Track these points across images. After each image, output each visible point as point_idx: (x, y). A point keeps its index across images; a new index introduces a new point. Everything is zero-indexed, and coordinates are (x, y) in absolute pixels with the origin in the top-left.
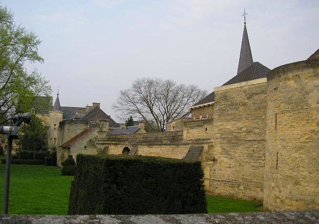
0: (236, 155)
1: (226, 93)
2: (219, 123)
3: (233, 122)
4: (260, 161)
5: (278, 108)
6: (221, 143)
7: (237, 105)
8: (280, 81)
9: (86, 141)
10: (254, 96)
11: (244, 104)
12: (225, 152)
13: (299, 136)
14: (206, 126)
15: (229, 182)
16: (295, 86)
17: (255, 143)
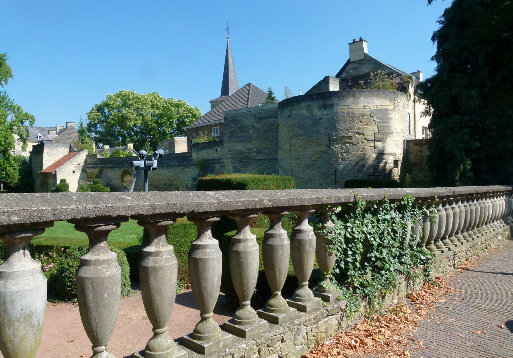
1: (236, 116)
2: (230, 145)
3: (243, 144)
6: (232, 163)
7: (246, 127)
8: (294, 109)
9: (73, 166)
10: (263, 120)
11: (254, 127)
13: (311, 156)
14: (216, 148)
16: (308, 114)
17: (264, 161)
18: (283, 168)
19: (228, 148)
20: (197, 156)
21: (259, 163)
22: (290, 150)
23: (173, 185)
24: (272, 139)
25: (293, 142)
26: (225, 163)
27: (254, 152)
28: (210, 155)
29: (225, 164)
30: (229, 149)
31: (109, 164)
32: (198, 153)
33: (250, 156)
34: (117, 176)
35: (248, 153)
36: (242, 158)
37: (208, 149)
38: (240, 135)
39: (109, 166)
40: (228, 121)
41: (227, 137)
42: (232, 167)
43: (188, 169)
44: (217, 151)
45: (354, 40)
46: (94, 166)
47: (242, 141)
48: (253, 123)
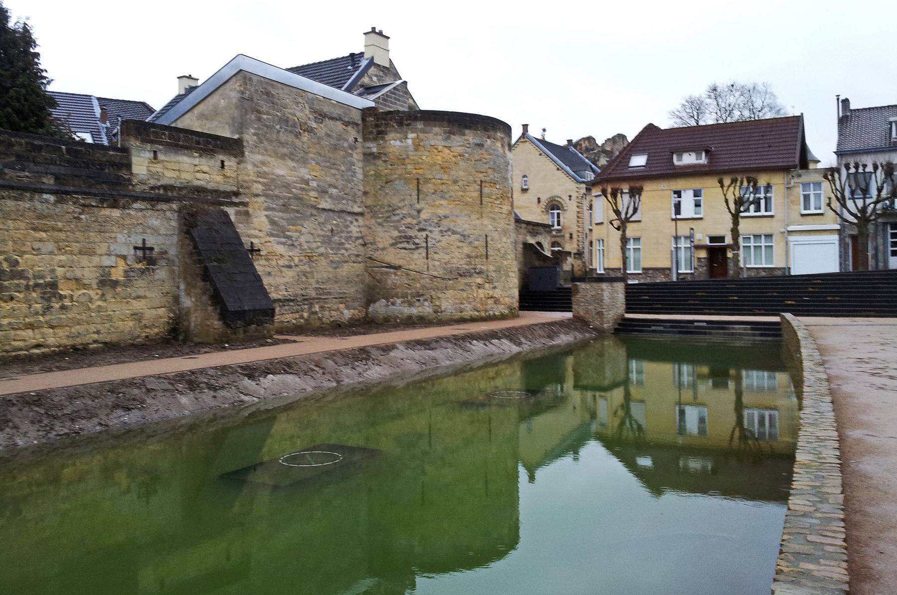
0: (302, 239)
2: (258, 158)
4: (343, 251)
5: (484, 174)
6: (268, 209)
8: (489, 138)
11: (310, 130)
12: (278, 230)
15: (292, 301)
17: (331, 214)
18: (454, 233)
19: (255, 165)
20: (158, 168)
21: (323, 216)
22: (481, 204)
23: (21, 275)
24: (343, 168)
25: (486, 190)
26: (250, 206)
27: (314, 190)
28: (199, 175)
29: (251, 210)
30: (256, 169)
32: (155, 158)
33: (305, 196)
35: (302, 189)
36: (289, 198)
37: (196, 154)
38: (283, 137)
40: (253, 89)
41: (254, 134)
42: (264, 219)
43: (116, 213)
44: (223, 166)
45: (374, 29)
47: (291, 156)
48: (309, 118)
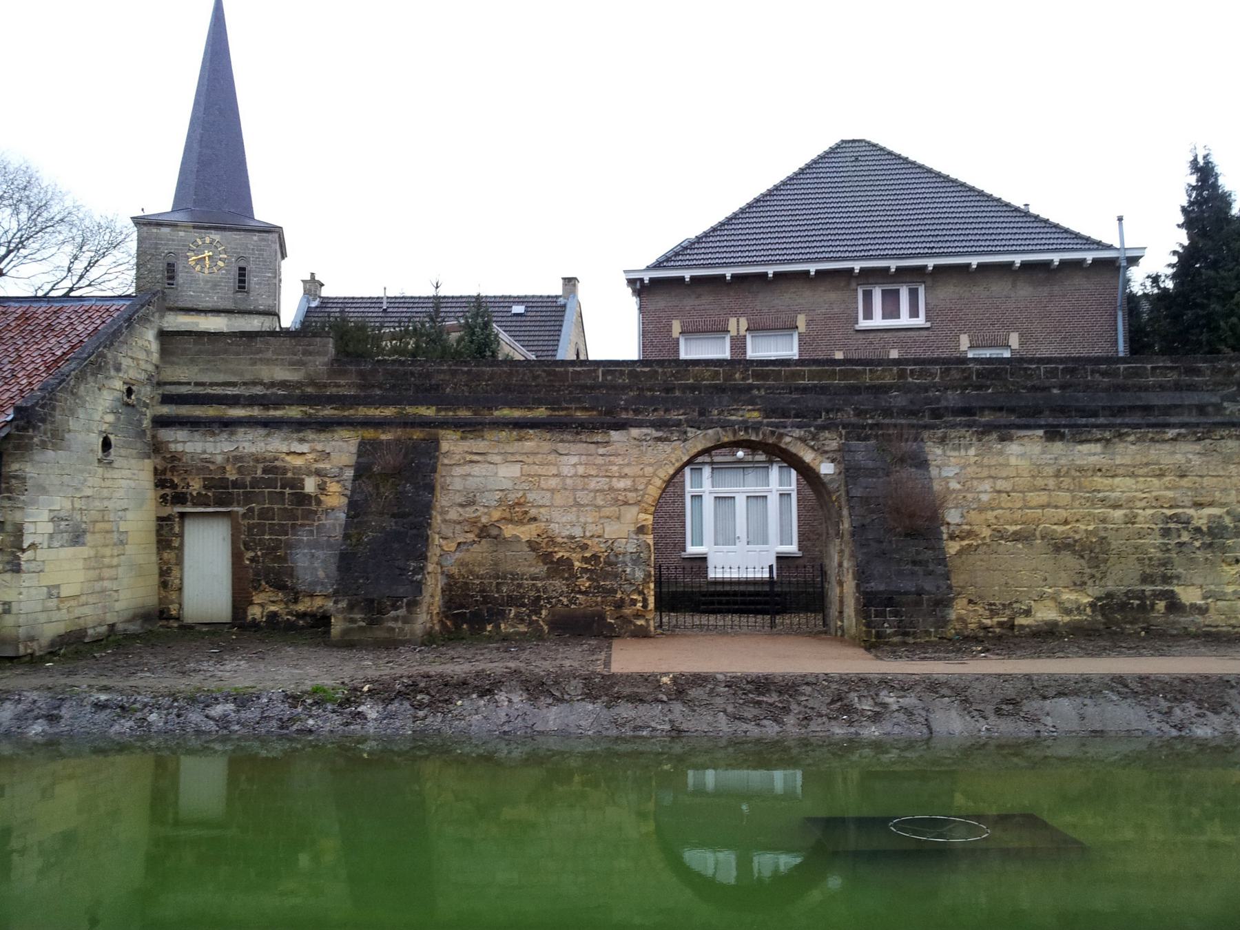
31: (511, 405)
34: (622, 484)
39: (506, 413)
46: (294, 412)
